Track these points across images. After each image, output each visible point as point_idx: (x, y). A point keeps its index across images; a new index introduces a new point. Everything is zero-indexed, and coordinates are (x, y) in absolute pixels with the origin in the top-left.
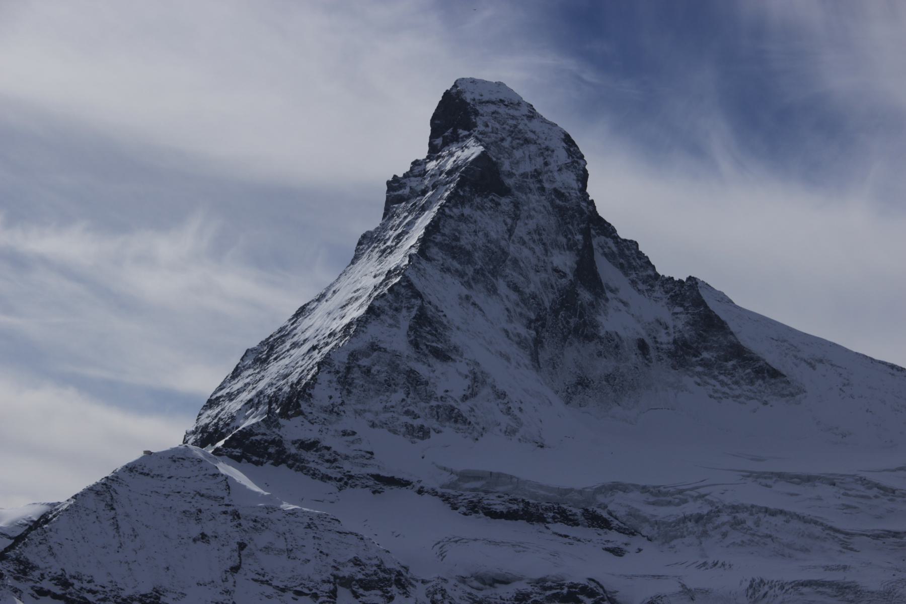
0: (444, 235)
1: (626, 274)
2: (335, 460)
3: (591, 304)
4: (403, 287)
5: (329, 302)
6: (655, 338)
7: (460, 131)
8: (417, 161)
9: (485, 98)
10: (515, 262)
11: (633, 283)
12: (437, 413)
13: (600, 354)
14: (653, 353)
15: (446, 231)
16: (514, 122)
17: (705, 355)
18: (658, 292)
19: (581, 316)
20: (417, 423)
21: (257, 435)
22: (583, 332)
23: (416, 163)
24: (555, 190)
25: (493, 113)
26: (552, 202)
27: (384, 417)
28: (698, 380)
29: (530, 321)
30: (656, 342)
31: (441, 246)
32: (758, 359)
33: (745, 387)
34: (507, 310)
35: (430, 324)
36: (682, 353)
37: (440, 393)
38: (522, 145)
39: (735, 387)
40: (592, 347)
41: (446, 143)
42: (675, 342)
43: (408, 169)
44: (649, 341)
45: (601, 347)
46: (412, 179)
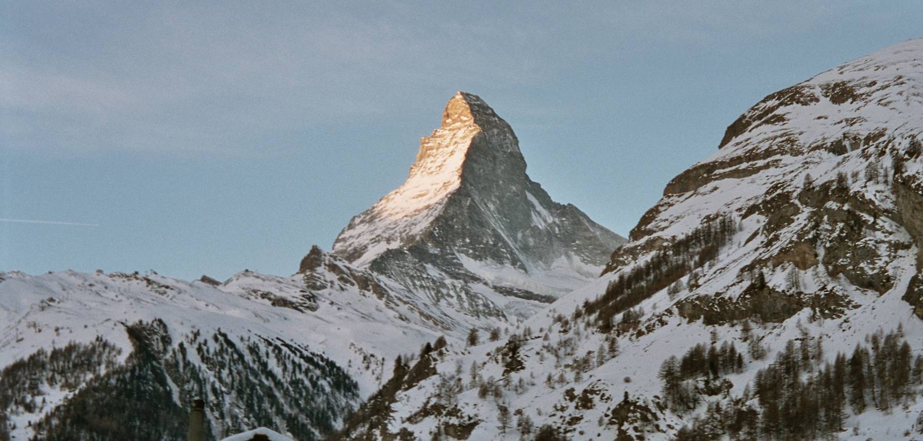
10: (498, 185)
36: (567, 240)
37: (484, 242)
41: (454, 121)
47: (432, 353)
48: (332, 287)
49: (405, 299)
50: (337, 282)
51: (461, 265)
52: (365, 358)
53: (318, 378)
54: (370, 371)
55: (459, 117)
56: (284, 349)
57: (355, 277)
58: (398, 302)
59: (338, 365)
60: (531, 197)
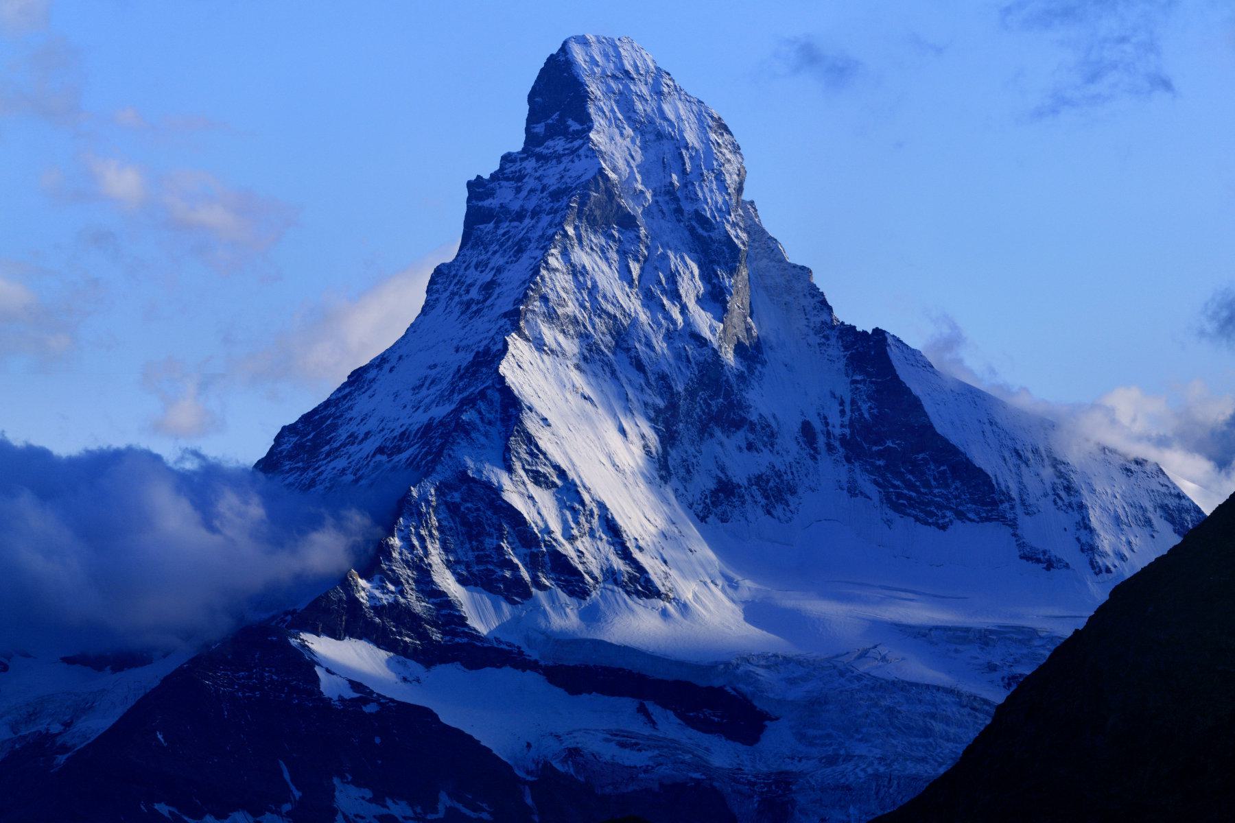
3: (741, 377)
6: (825, 418)
7: (570, 122)
8: (509, 154)
13: (750, 447)
14: (821, 440)
18: (835, 349)
19: (727, 396)
23: (507, 159)
24: (696, 211)
26: (692, 230)
29: (658, 411)
40: (740, 437)
41: (551, 133)
42: (851, 425)
43: (497, 167)
44: (818, 425)
45: (751, 437)
46: (504, 183)
55: (562, 119)
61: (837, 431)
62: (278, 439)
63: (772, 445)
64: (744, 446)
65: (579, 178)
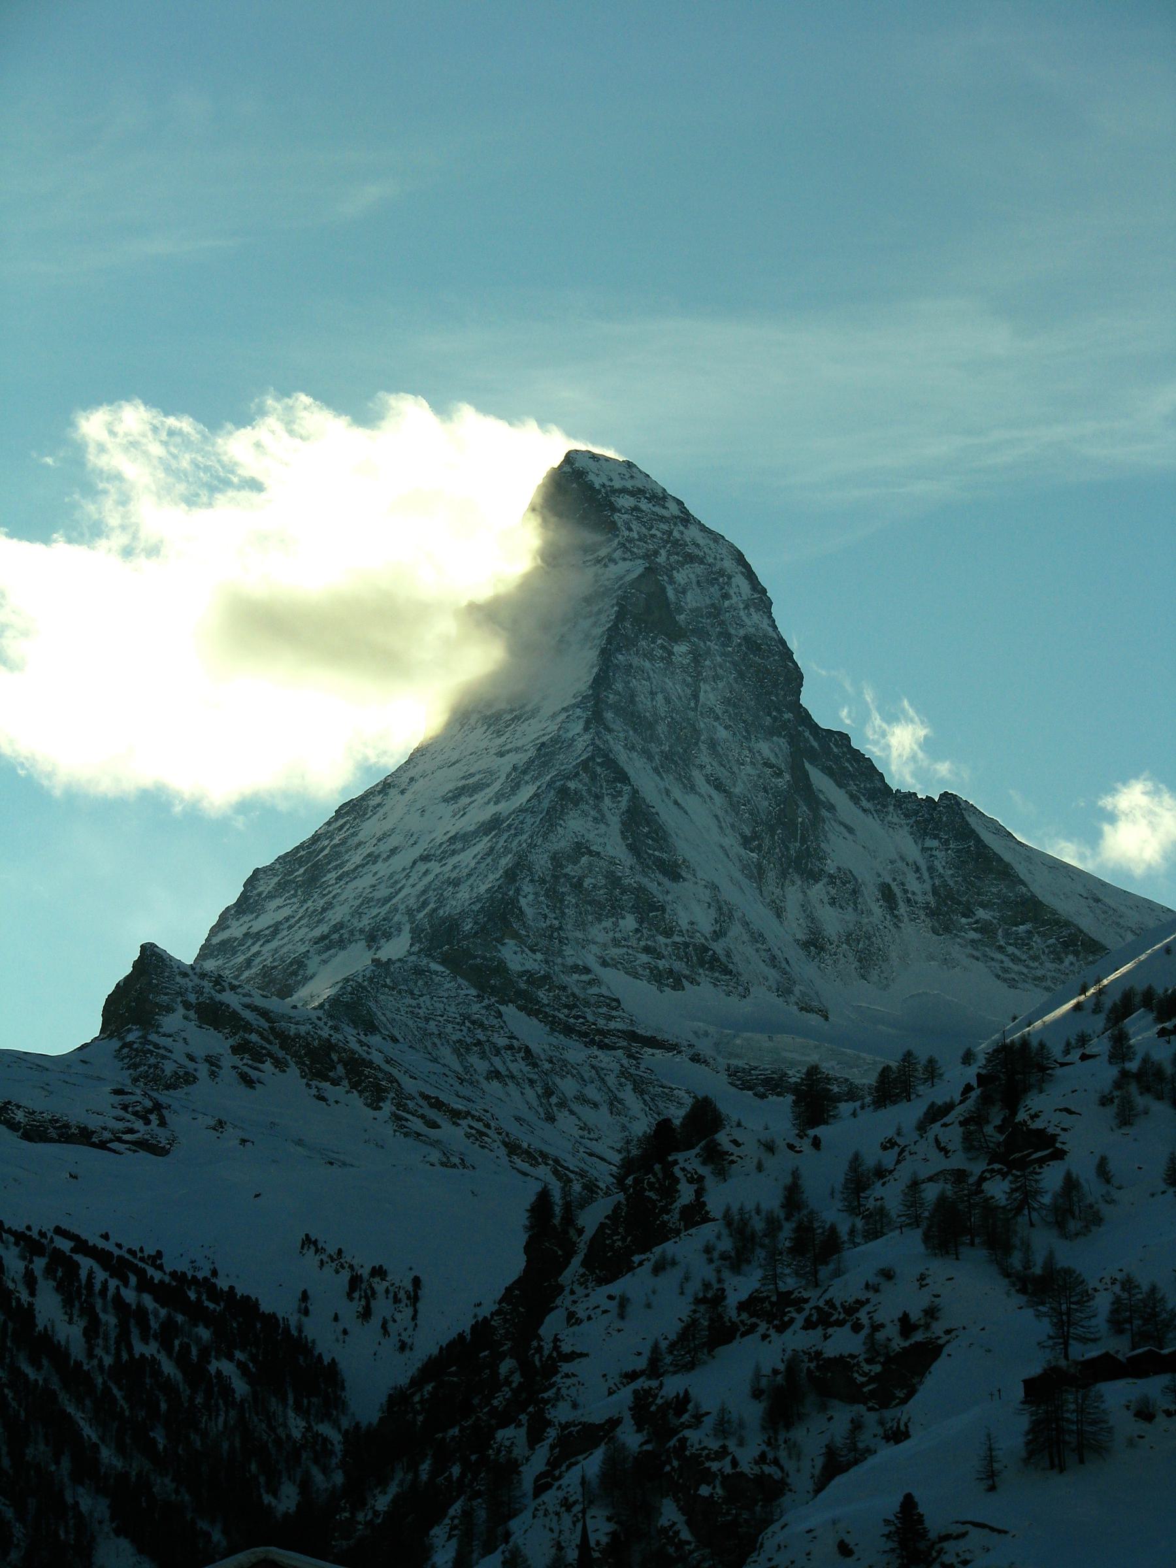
0: (617, 693)
1: (840, 785)
2: (575, 1006)
4: (598, 764)
5: (408, 796)
6: (903, 884)
9: (617, 484)
10: (713, 745)
11: (854, 798)
12: (686, 954)
13: (833, 902)
14: (902, 909)
15: (619, 686)
16: (665, 527)
17: (981, 914)
19: (804, 840)
20: (662, 964)
21: (475, 957)
22: (806, 864)
24: (746, 638)
25: (636, 509)
27: (615, 952)
28: (975, 953)
30: (906, 891)
31: (618, 710)
32: (1068, 924)
33: (1048, 965)
34: (716, 816)
35: (648, 825)
36: (945, 911)
37: (684, 924)
38: (682, 565)
39: (1032, 964)
42: (935, 891)
47: (680, 1157)
48: (213, 1075)
49: (459, 1105)
50: (229, 1060)
51: (614, 1003)
52: (355, 1282)
53: (205, 1354)
54: (375, 1321)
56: (86, 1263)
57: (285, 1040)
58: (432, 1114)
59: (266, 1307)
60: (819, 779)
61: (920, 899)
62: (251, 883)
63: (855, 904)
64: (826, 900)
65: (621, 578)
